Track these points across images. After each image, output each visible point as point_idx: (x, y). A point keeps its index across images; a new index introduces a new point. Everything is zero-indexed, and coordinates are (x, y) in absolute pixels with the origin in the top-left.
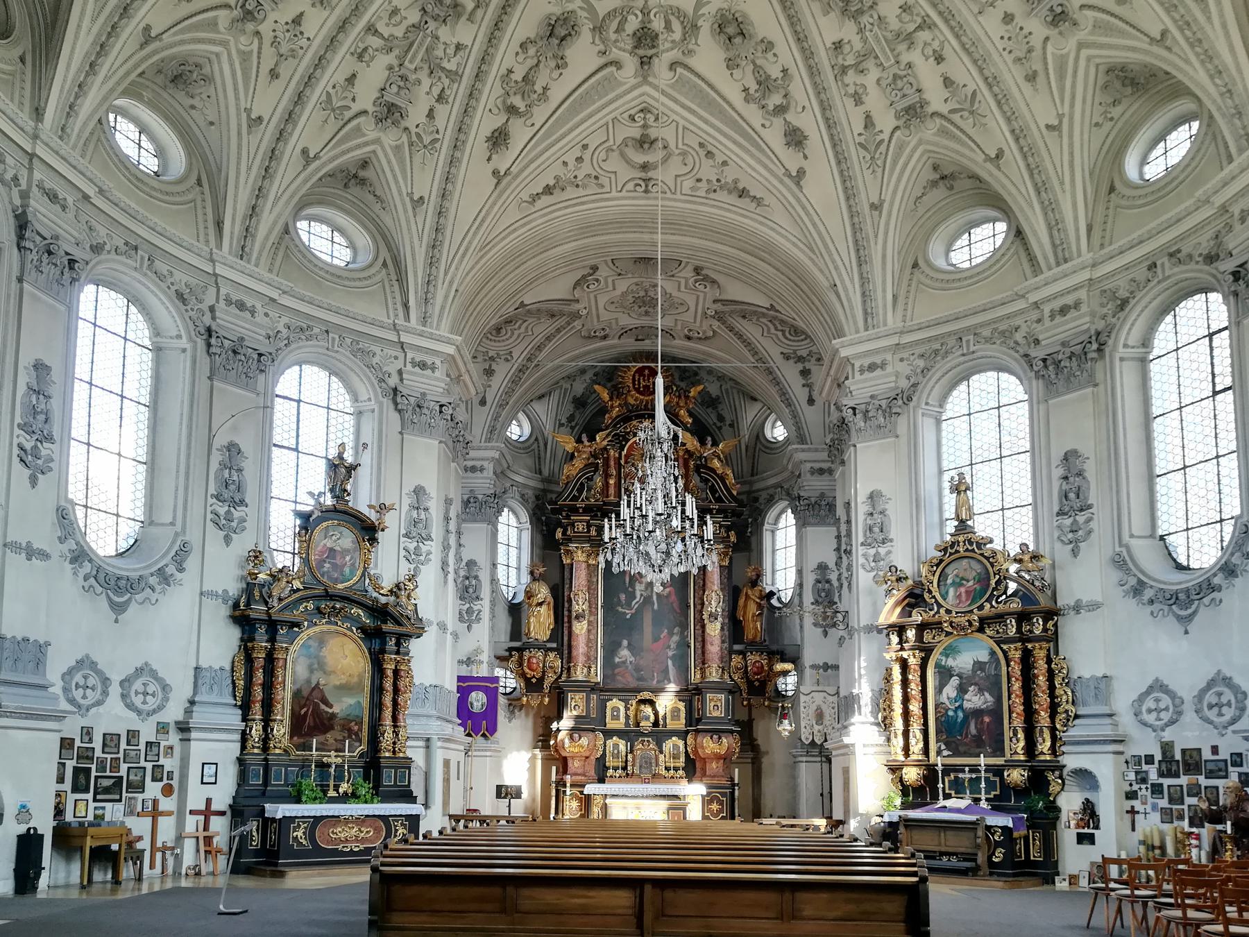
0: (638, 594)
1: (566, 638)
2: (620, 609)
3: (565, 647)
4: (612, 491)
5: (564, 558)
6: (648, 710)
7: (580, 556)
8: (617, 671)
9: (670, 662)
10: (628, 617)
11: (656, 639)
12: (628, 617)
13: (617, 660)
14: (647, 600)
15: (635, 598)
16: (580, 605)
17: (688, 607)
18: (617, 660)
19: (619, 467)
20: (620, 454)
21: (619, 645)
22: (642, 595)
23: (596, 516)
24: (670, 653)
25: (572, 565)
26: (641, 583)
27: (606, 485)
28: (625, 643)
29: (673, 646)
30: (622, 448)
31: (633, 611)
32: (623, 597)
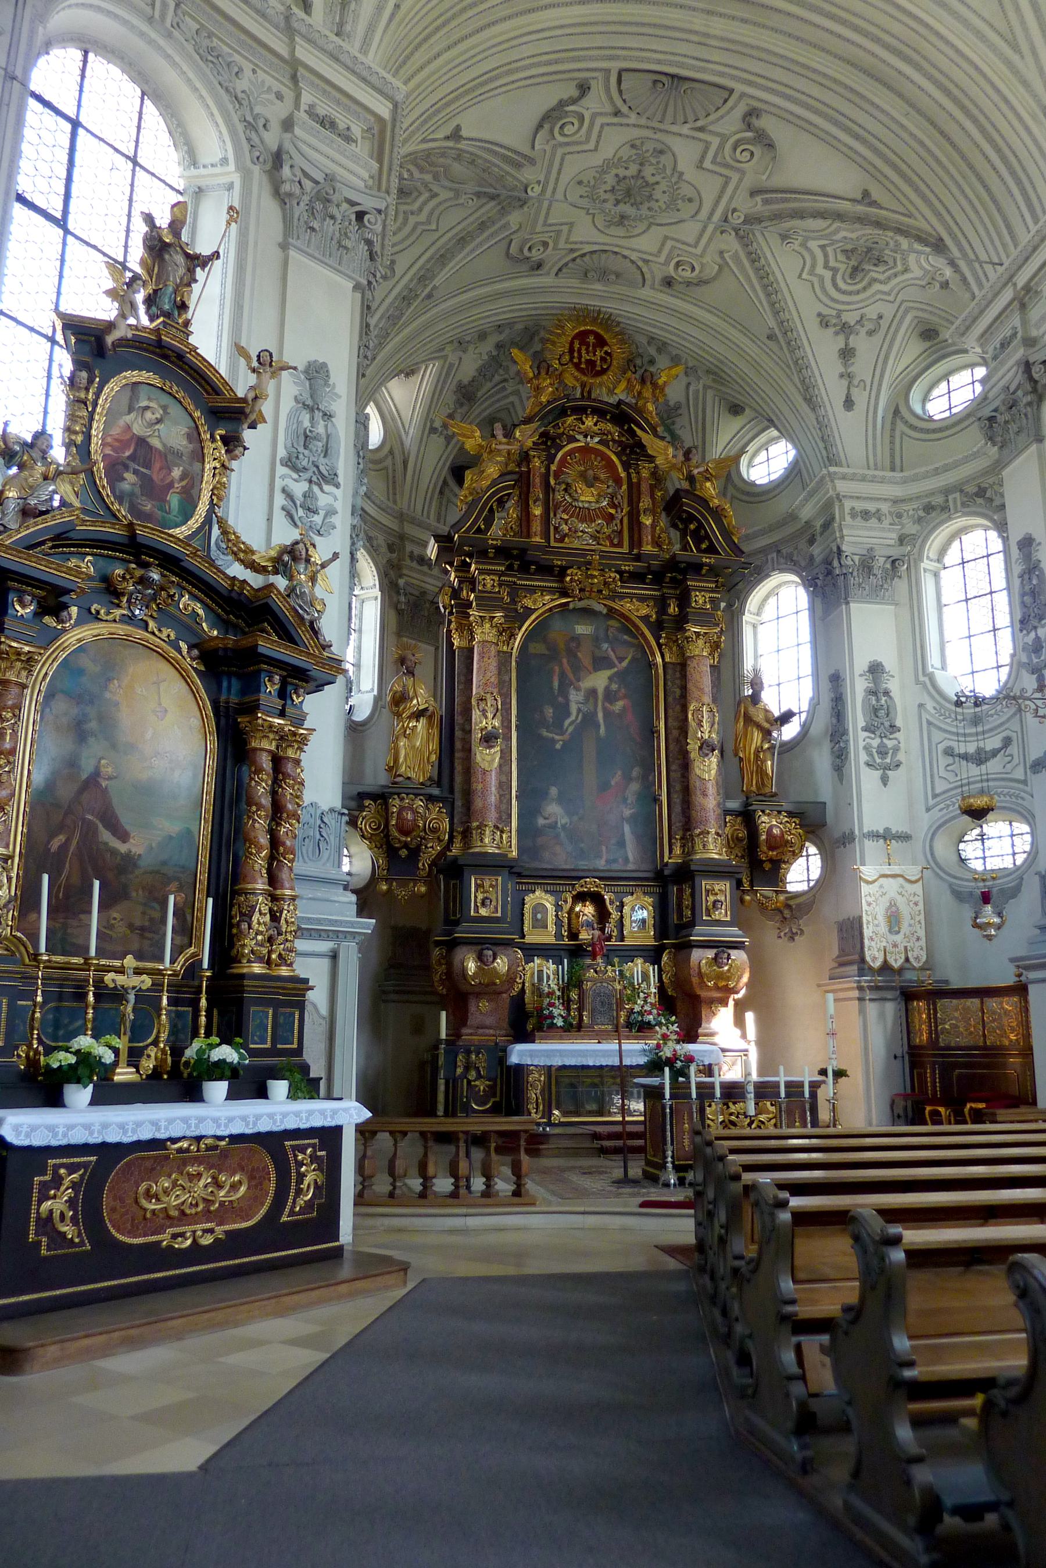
0: (574, 708)
1: (458, 779)
2: (545, 733)
3: (458, 795)
4: (536, 526)
5: (455, 636)
6: (588, 910)
7: (484, 633)
8: (540, 841)
9: (627, 829)
10: (558, 746)
11: (604, 787)
12: (558, 746)
13: (541, 821)
14: (588, 720)
15: (569, 715)
16: (483, 720)
17: (653, 732)
18: (541, 821)
19: (547, 488)
20: (548, 469)
21: (544, 795)
22: (579, 710)
23: (510, 568)
24: (627, 812)
25: (471, 650)
26: (578, 689)
27: (526, 517)
28: (554, 791)
29: (631, 799)
30: (551, 459)
31: (566, 737)
32: (549, 712)
